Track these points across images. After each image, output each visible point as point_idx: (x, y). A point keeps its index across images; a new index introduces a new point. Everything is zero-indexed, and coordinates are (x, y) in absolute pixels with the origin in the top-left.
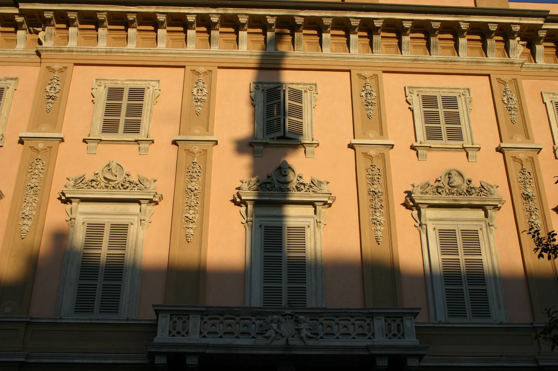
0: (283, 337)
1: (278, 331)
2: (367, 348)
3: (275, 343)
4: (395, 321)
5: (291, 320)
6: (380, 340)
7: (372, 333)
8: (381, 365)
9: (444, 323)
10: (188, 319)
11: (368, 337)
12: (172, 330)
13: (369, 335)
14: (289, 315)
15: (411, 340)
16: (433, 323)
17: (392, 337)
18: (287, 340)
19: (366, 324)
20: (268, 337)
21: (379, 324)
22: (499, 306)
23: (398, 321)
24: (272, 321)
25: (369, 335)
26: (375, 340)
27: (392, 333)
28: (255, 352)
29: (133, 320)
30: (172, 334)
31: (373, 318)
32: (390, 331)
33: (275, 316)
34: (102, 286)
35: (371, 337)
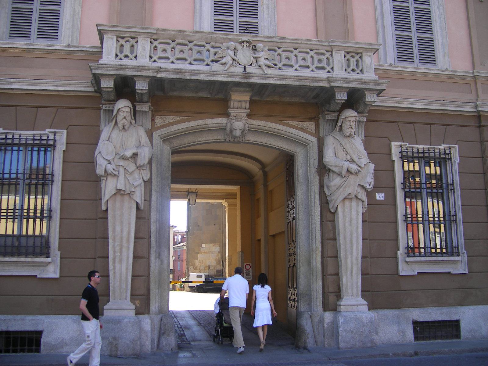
0: (239, 64)
1: (235, 58)
2: (328, 80)
3: (232, 70)
4: (353, 57)
5: (248, 48)
6: (339, 72)
7: (331, 66)
8: (340, 98)
9: (395, 67)
10: (137, 42)
11: (327, 71)
12: (118, 53)
13: (328, 69)
14: (247, 42)
15: (370, 75)
16: (384, 66)
17: (351, 72)
18: (245, 66)
19: (325, 57)
20: (224, 64)
21: (339, 58)
22: (444, 55)
23: (357, 57)
24: (228, 48)
25: (328, 69)
26: (334, 73)
27: (351, 68)
28: (211, 78)
29: (74, 46)
30: (118, 58)
31: (332, 52)
32: (348, 66)
33: (232, 43)
34: (38, 11)
35: (331, 71)
